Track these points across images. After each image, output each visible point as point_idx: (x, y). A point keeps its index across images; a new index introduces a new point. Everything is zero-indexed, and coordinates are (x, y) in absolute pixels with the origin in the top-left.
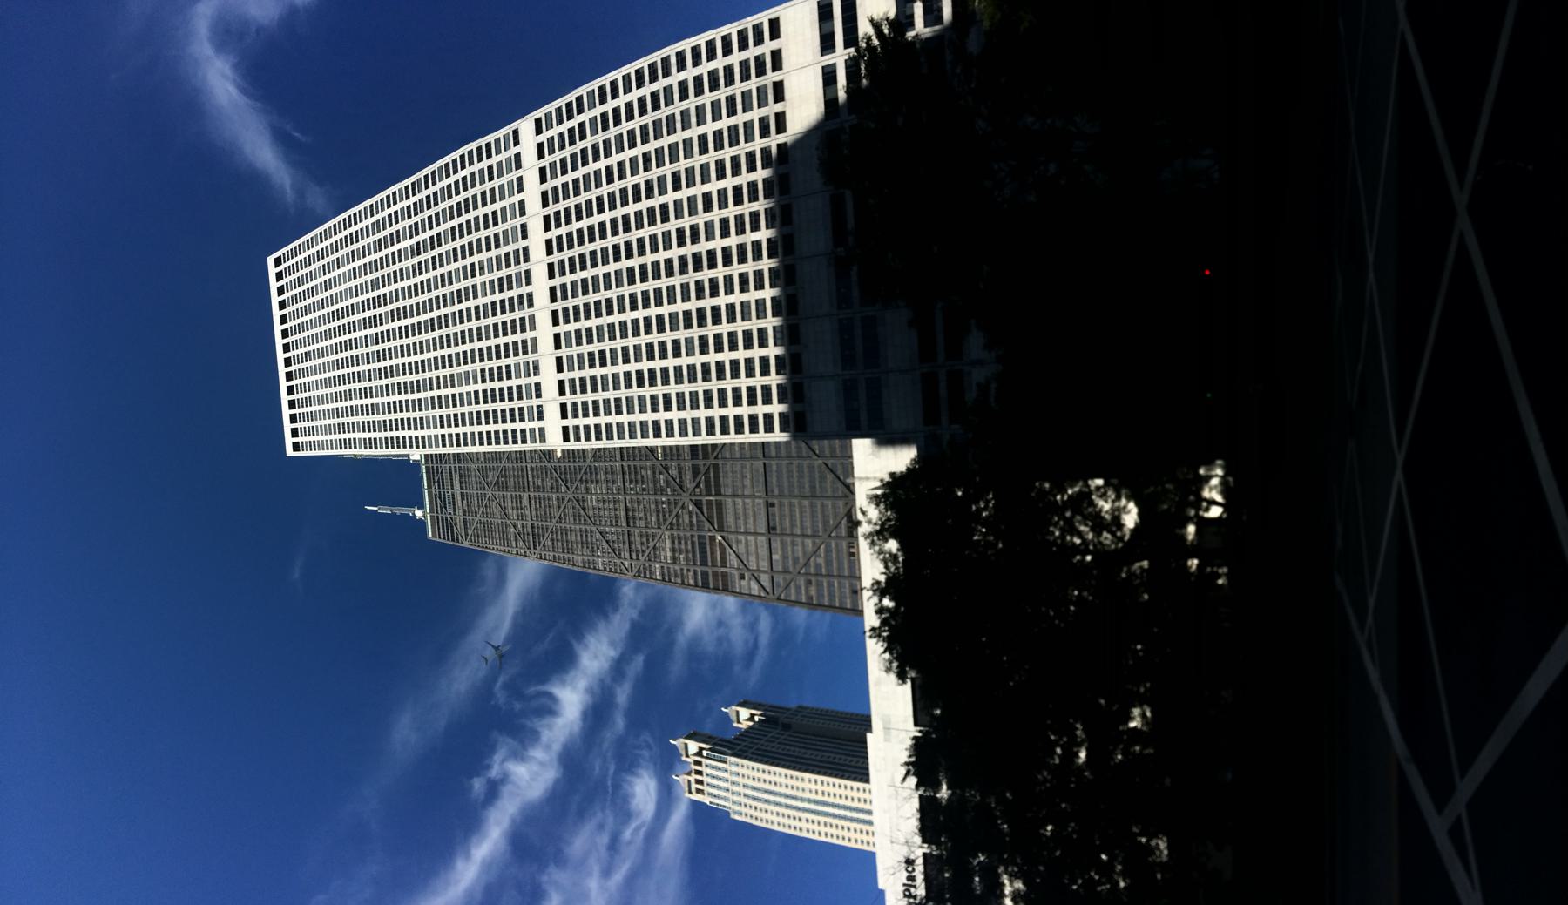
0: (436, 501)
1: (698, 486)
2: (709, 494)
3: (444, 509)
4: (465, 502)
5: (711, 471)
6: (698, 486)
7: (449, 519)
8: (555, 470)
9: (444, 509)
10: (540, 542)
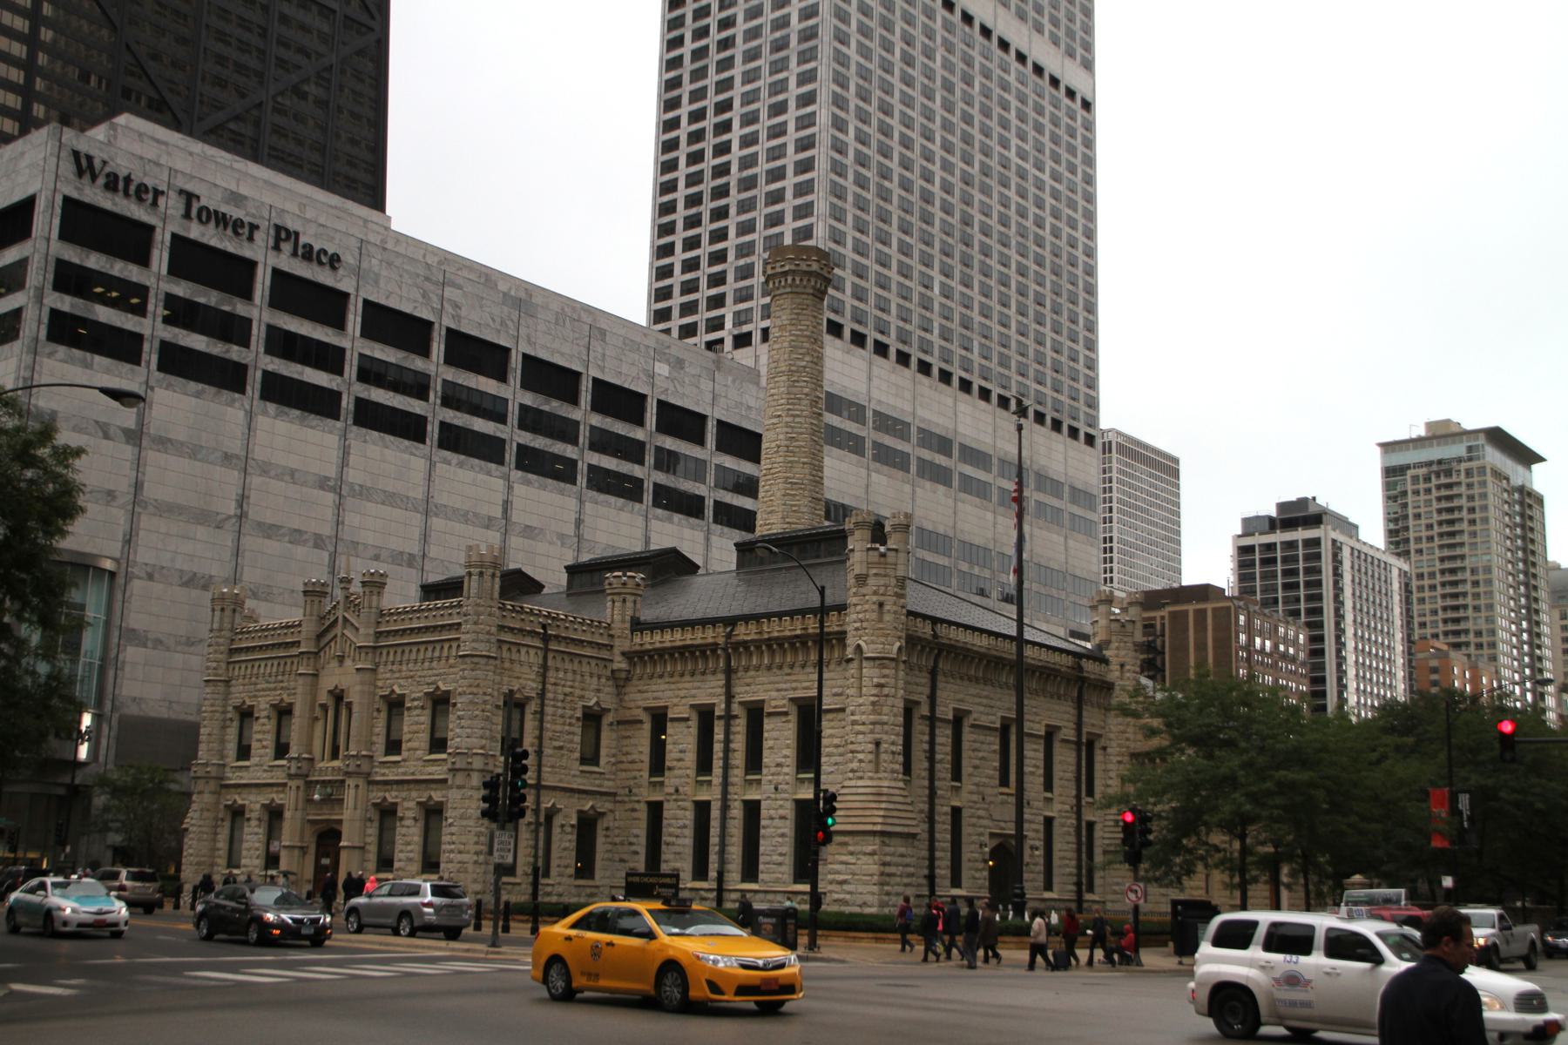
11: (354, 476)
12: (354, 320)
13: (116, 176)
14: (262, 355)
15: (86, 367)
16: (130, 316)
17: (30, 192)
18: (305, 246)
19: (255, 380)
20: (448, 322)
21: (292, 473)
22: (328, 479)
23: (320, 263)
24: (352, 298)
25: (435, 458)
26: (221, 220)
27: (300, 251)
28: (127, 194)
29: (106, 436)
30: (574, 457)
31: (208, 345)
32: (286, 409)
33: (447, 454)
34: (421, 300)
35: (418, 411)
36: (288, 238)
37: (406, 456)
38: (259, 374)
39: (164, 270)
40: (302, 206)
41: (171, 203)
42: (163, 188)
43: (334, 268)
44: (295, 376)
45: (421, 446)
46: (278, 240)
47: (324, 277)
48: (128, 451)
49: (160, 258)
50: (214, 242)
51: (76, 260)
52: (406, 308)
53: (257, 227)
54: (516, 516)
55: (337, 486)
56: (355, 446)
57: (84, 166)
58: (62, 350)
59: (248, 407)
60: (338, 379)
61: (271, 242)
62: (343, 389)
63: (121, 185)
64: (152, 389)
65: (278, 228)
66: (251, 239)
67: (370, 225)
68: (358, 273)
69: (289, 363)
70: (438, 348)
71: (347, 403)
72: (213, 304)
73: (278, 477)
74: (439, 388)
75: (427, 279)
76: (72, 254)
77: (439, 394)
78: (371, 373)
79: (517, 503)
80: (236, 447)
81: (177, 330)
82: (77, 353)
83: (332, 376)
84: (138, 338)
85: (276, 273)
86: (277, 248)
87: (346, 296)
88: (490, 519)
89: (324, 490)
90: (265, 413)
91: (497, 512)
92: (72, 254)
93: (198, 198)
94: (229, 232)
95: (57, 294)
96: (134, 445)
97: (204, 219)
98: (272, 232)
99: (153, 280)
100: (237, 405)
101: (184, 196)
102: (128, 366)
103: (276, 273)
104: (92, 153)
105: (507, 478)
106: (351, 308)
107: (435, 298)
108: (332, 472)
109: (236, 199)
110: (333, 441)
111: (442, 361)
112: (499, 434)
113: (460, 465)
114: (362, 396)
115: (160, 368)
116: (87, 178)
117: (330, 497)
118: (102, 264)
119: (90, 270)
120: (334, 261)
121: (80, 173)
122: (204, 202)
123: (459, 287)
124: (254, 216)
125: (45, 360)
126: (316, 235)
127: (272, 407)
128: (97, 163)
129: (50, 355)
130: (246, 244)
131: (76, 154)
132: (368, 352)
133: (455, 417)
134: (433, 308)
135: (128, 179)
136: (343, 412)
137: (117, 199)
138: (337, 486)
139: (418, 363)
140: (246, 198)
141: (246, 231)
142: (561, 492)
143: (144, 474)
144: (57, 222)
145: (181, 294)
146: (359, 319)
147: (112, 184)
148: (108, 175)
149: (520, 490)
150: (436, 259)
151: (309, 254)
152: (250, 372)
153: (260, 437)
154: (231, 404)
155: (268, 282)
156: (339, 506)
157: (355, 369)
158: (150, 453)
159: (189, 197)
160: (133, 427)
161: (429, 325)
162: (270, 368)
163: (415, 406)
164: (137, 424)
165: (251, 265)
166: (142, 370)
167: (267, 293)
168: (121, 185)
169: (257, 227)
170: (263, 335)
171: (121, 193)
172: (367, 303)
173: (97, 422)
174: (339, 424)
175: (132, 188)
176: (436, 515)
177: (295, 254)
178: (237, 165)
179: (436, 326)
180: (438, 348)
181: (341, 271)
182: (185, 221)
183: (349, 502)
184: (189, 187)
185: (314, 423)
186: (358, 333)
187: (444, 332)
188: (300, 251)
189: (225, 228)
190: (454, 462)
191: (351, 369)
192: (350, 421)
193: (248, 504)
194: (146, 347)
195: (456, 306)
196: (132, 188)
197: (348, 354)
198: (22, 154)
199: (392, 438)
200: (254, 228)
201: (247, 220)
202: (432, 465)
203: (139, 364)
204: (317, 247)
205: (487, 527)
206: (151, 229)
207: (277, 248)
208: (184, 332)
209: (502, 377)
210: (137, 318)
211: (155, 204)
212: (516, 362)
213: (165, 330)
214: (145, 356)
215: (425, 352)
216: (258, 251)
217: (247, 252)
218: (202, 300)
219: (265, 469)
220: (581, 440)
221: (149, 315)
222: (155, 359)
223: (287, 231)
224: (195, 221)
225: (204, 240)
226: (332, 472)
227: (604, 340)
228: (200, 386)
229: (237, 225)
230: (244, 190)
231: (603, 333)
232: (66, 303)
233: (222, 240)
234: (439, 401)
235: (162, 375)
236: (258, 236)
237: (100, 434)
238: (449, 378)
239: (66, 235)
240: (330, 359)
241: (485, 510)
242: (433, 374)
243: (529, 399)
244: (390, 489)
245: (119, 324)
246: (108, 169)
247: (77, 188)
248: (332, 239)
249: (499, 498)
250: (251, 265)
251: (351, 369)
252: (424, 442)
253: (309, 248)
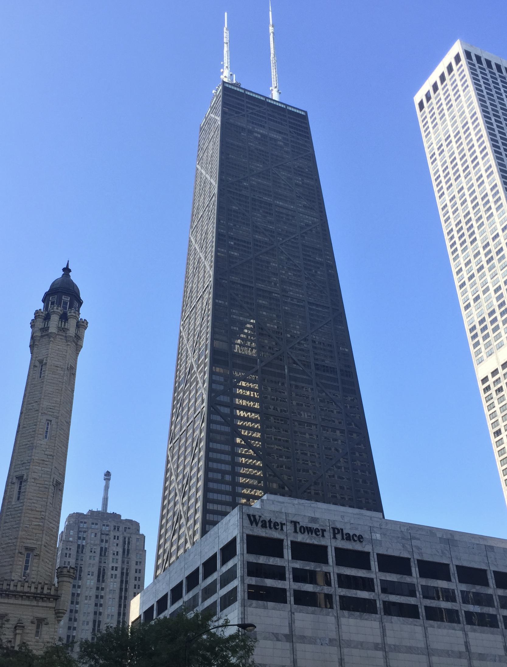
0: (257, 106)
1: (295, 363)
2: (290, 370)
3: (251, 111)
4: (259, 136)
5: (307, 378)
6: (295, 363)
7: (244, 113)
8: (294, 238)
9: (251, 111)
10: (234, 198)
11: (390, 641)
12: (374, 564)
13: (265, 521)
14: (337, 589)
15: (265, 609)
16: (279, 581)
17: (234, 536)
18: (346, 534)
19: (336, 600)
20: (416, 557)
21: (362, 643)
22: (378, 644)
23: (355, 541)
24: (371, 554)
25: (426, 625)
26: (309, 530)
27: (345, 537)
28: (270, 528)
29: (278, 640)
30: (494, 613)
31: (313, 588)
32: (353, 613)
33: (431, 622)
34: (402, 549)
35: (413, 603)
36: (338, 533)
37: (413, 626)
38: (338, 598)
39: (290, 558)
40: (342, 517)
41: (288, 528)
42: (284, 522)
43: (361, 542)
44: (354, 596)
45: (418, 620)
46: (334, 535)
47: (357, 547)
48: (288, 645)
49: (287, 553)
50: (308, 541)
51: (255, 561)
52: (396, 554)
53: (325, 530)
54: (473, 649)
55: (382, 647)
56: (388, 625)
57: (253, 520)
58: (254, 602)
59: (336, 615)
60: (373, 594)
61: (332, 536)
62: (376, 598)
63: (268, 525)
64: (294, 613)
65: (334, 529)
66: (323, 536)
67: (373, 519)
68: (372, 541)
69: (350, 590)
70: (415, 570)
71: (379, 605)
72: (312, 569)
73: (355, 647)
74: (420, 589)
75: (403, 538)
76: (252, 558)
77: (421, 593)
78: (387, 588)
79: (472, 642)
80: (333, 635)
81: (299, 584)
82: (260, 602)
83: (370, 593)
84: (284, 591)
85: (337, 549)
86: (335, 537)
87: (368, 553)
88: (460, 653)
89: (378, 650)
90: (344, 616)
91: (463, 649)
92: (252, 558)
93: (299, 523)
94: (314, 535)
95: (250, 577)
96: (290, 642)
98: (331, 531)
99: (287, 563)
100: (331, 614)
101: (293, 523)
102: (282, 605)
103: (337, 549)
104: (255, 514)
105: (463, 630)
106: (371, 558)
107: (408, 547)
108: (379, 640)
109: (314, 520)
110: (376, 624)
111: (418, 576)
112: (454, 608)
113: (439, 627)
114: (385, 600)
115: (295, 604)
116: (254, 524)
117: (380, 654)
118: (265, 560)
119: (261, 564)
120: (360, 538)
122: (301, 524)
123: (419, 539)
124: (322, 526)
125: (249, 608)
126: (350, 529)
127: (346, 613)
128: (257, 517)
129: (250, 606)
130: (321, 538)
131: (249, 516)
132: (383, 578)
133: (431, 603)
134: (409, 551)
135: (270, 521)
136: (378, 609)
137: (267, 531)
138: (382, 647)
139: (407, 579)
140: (318, 518)
142: (493, 633)
143: (296, 655)
144: (245, 546)
145: (299, 567)
146: (376, 563)
147: (264, 526)
148: (262, 522)
149: (471, 635)
150: (406, 528)
151: (349, 538)
152: (334, 597)
153: (344, 628)
154: (328, 615)
155: (334, 554)
156: (386, 658)
157: (379, 587)
158: (298, 645)
159: (295, 523)
160: (288, 633)
161: (409, 559)
162: (342, 594)
163: (411, 601)
164: (289, 630)
165: (325, 548)
166: (288, 606)
167: (334, 559)
168: (268, 525)
169: (325, 530)
170: (336, 579)
171: (268, 528)
172: (378, 555)
173: (273, 633)
174: (378, 616)
175: (272, 525)
176: (434, 655)
177: (343, 539)
178: (313, 505)
179: (412, 559)
180: (415, 570)
181: (364, 543)
182: (295, 534)
183: (391, 655)
184: (294, 519)
185: (366, 617)
186: (377, 570)
187: (416, 562)
189: (312, 534)
190: (436, 626)
191: (378, 588)
192: (383, 614)
193: (344, 663)
194: (288, 594)
195: (419, 548)
196: (272, 525)
197: (375, 580)
198: (230, 520)
199: (404, 618)
200: (323, 531)
201: (319, 528)
202: (425, 629)
203: (286, 603)
204: (351, 534)
205: (460, 657)
206: (282, 541)
207: (335, 537)
208: (303, 584)
209: (448, 579)
210: (282, 582)
211: (282, 529)
212: (453, 570)
213: (295, 585)
214: (288, 599)
215: (410, 574)
217: (323, 542)
218: (308, 568)
219: (349, 644)
220: (496, 604)
221: (287, 579)
222: (292, 598)
223: (338, 529)
224: (299, 533)
225: (304, 541)
226: (379, 640)
227: (494, 551)
228: (313, 608)
229: (316, 531)
230: (317, 515)
231: (492, 548)
232: (253, 581)
233: (311, 539)
234: (421, 596)
235: (296, 606)
236: (325, 534)
237: (275, 639)
238: (424, 584)
239: (250, 551)
240: (367, 585)
241: (456, 649)
242: (416, 583)
243: (464, 587)
244: (408, 645)
245: (275, 586)
246: (261, 519)
247: (250, 530)
248: (357, 529)
249: (462, 641)
250: (325, 548)
251: (378, 588)
252: (419, 618)
253: (348, 534)
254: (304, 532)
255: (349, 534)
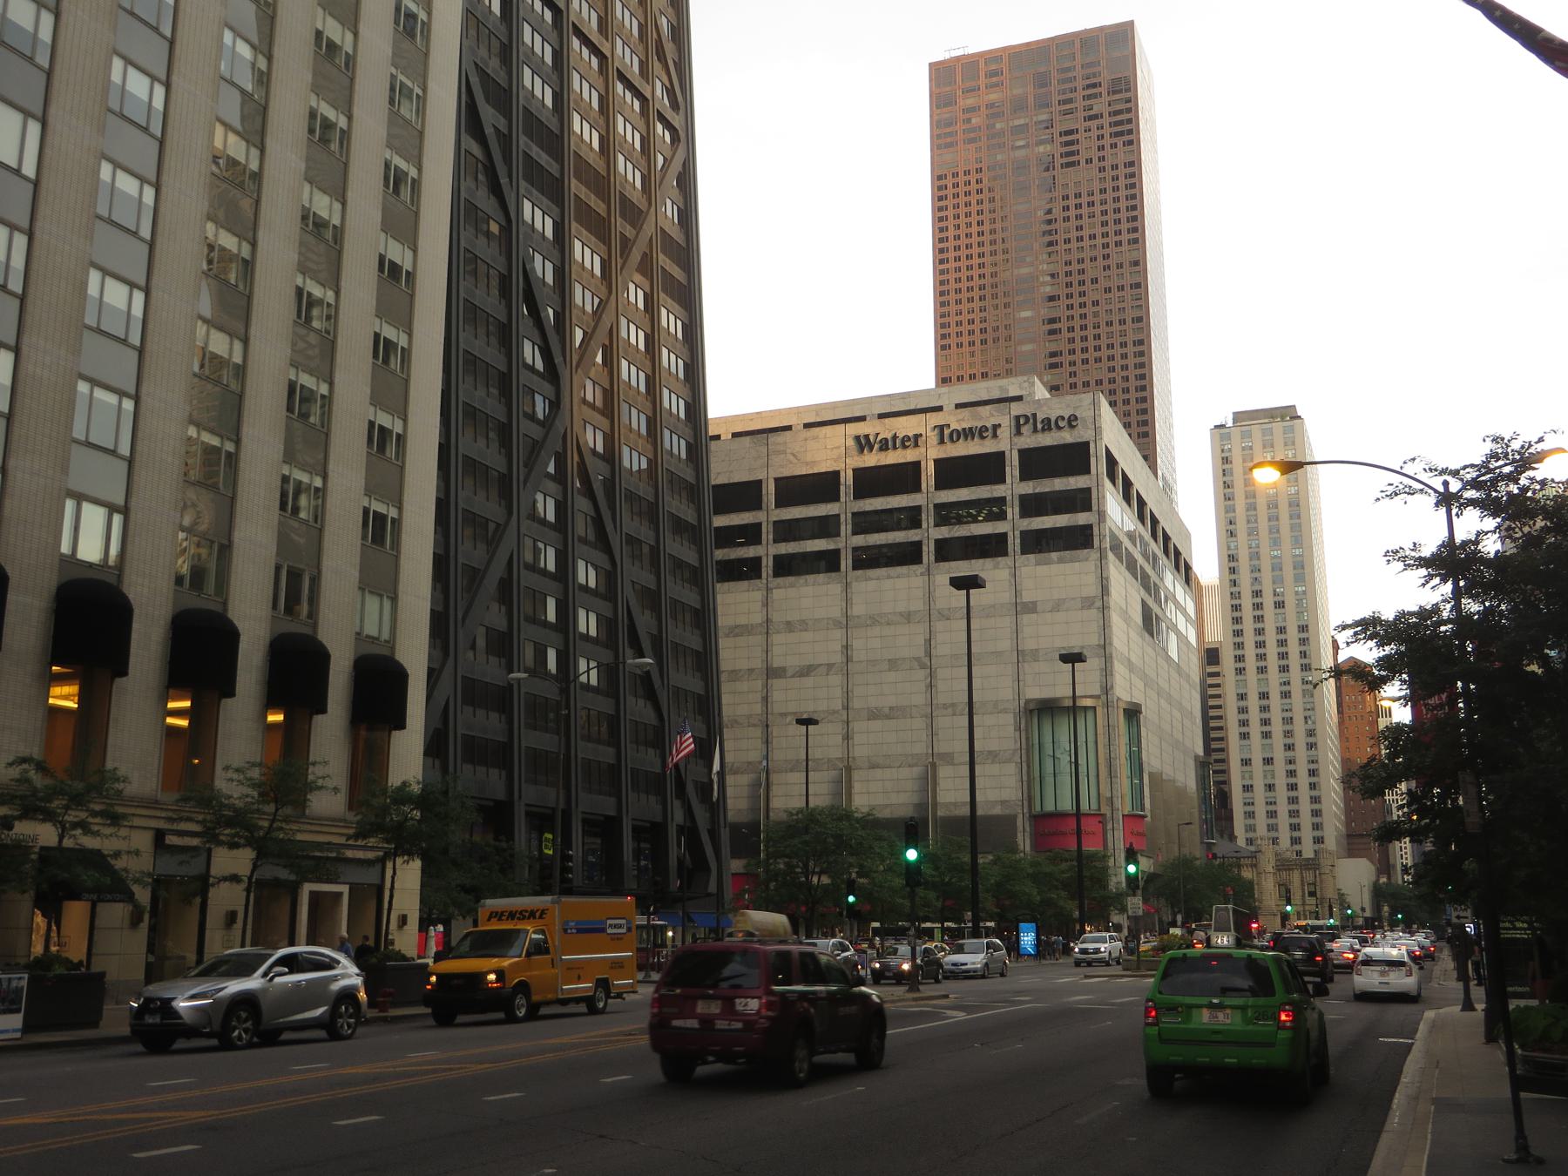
18: (1043, 421)
23: (1059, 428)
27: (1039, 426)
43: (1072, 427)
47: (1067, 437)
61: (1014, 431)
66: (995, 436)
97: (955, 439)
121: (861, 450)
128: (872, 438)
135: (895, 437)
141: (990, 433)
151: (1048, 425)
154: (996, 567)
177: (1035, 430)
188: (1039, 426)
189: (973, 438)
207: (1019, 433)
216: (1005, 443)
254: (958, 440)
255: (1049, 420)
